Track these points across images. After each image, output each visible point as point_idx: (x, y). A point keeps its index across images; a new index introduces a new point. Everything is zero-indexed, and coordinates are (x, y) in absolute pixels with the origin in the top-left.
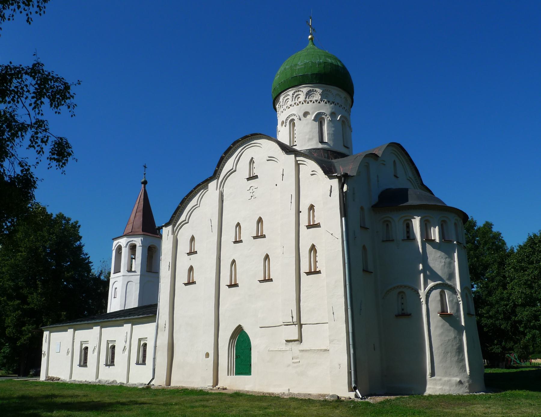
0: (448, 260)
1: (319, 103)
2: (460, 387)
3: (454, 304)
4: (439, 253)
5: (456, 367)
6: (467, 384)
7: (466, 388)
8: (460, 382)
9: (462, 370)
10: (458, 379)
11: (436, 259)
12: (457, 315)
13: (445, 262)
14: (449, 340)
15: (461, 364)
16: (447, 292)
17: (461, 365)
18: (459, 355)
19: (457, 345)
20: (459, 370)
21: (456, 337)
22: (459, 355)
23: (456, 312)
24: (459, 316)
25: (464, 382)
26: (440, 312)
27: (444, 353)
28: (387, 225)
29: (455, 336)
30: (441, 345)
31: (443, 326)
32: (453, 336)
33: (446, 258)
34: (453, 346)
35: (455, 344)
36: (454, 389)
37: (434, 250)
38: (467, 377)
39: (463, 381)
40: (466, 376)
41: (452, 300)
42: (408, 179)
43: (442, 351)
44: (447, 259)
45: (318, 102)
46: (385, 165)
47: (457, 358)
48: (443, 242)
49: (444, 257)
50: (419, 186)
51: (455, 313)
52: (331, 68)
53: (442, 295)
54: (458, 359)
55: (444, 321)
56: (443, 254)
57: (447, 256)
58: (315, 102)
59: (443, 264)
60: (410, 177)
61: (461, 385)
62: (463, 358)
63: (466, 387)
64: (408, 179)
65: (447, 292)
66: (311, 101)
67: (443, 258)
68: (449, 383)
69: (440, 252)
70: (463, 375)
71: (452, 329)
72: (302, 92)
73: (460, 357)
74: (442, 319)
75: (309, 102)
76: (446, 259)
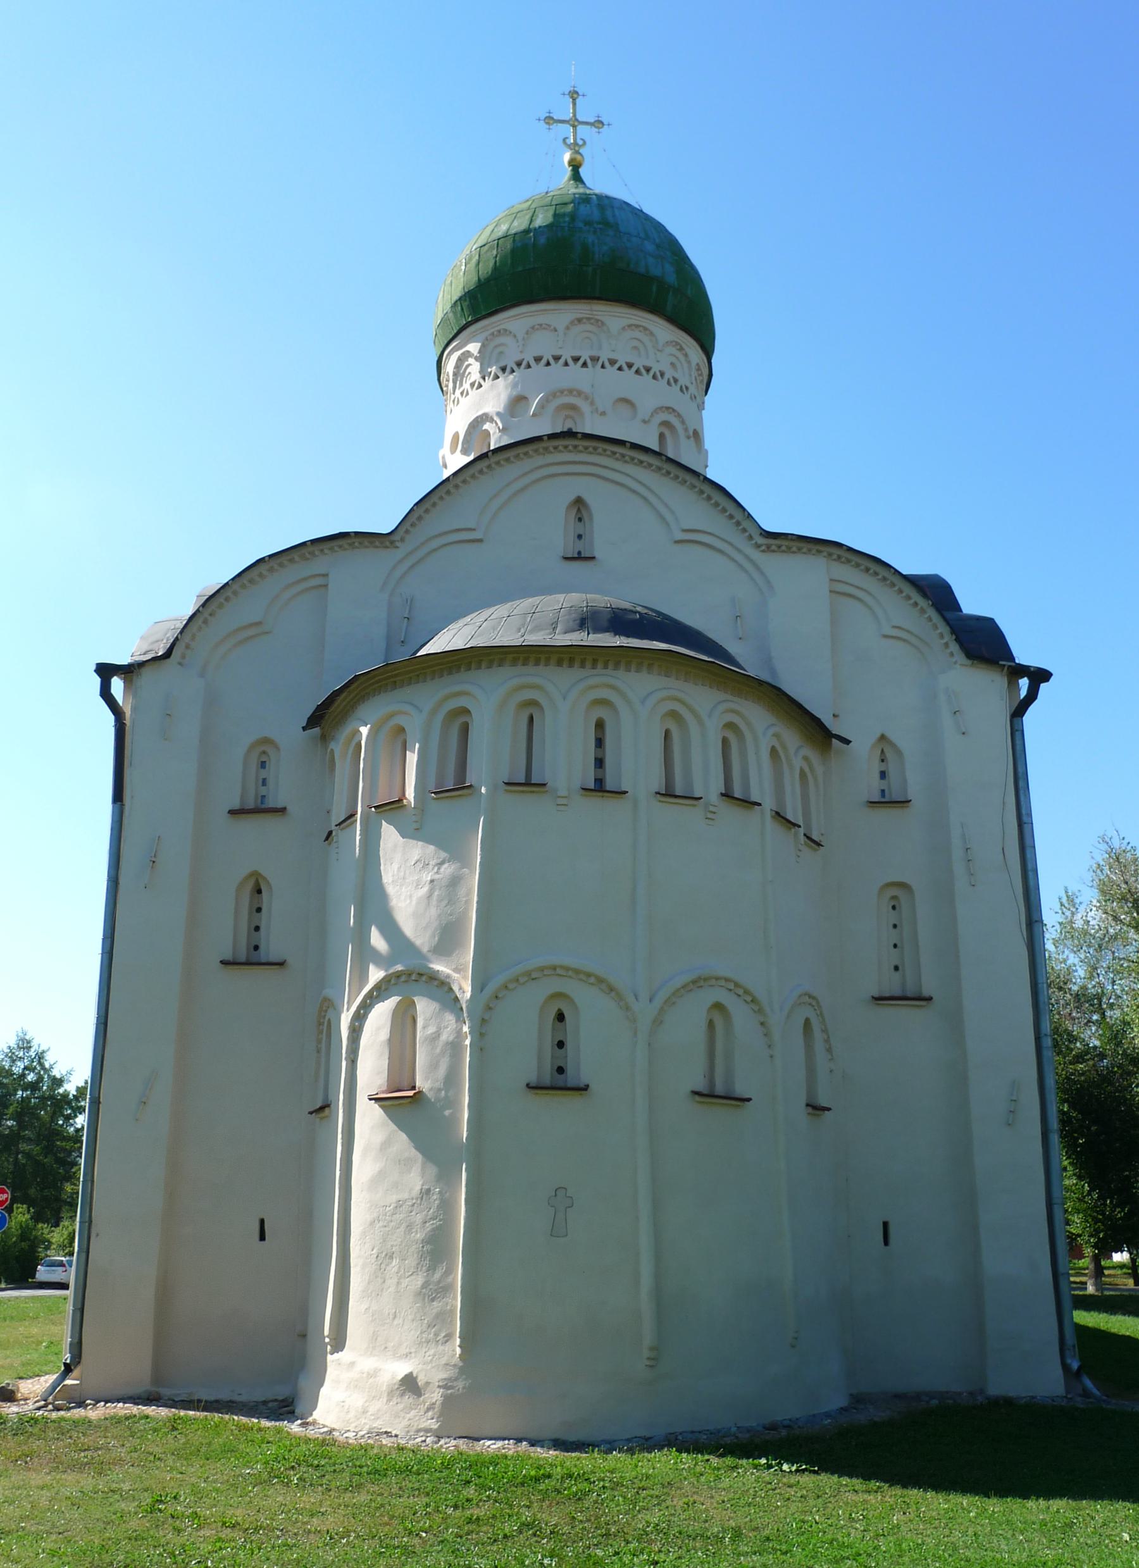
0: (448, 869)
2: (401, 1406)
3: (438, 1050)
4: (418, 850)
5: (410, 1317)
6: (435, 1396)
7: (430, 1414)
8: (410, 1385)
9: (436, 1335)
10: (401, 1369)
11: (404, 878)
12: (446, 1097)
13: (432, 881)
14: (399, 1204)
15: (437, 1305)
16: (424, 1007)
17: (435, 1311)
18: (432, 1269)
19: (428, 1224)
20: (421, 1333)
21: (428, 1191)
22: (432, 1269)
23: (444, 1084)
24: (453, 1103)
25: (428, 1383)
26: (385, 1088)
27: (377, 1257)
29: (426, 1187)
30: (372, 1223)
31: (385, 1145)
32: (418, 1188)
33: (442, 863)
34: (410, 1227)
35: (419, 1218)
36: (379, 1410)
37: (405, 840)
38: (447, 1364)
39: (421, 1381)
40: (444, 1361)
41: (437, 1036)
42: (677, 542)
43: (373, 1250)
44: (446, 865)
46: (480, 541)
47: (419, 1281)
48: (435, 799)
49: (432, 863)
50: (758, 546)
51: (439, 1090)
52: (496, 257)
53: (404, 1019)
54: (425, 1285)
55: (393, 1127)
56: (432, 848)
57: (443, 855)
59: (426, 889)
61: (408, 1399)
62: (450, 1279)
63: (428, 1410)
64: (677, 542)
65: (424, 1007)
68: (371, 1380)
69: (420, 843)
70: (431, 1352)
71: (420, 1156)
73: (437, 1276)
74: (387, 1118)
76: (439, 869)
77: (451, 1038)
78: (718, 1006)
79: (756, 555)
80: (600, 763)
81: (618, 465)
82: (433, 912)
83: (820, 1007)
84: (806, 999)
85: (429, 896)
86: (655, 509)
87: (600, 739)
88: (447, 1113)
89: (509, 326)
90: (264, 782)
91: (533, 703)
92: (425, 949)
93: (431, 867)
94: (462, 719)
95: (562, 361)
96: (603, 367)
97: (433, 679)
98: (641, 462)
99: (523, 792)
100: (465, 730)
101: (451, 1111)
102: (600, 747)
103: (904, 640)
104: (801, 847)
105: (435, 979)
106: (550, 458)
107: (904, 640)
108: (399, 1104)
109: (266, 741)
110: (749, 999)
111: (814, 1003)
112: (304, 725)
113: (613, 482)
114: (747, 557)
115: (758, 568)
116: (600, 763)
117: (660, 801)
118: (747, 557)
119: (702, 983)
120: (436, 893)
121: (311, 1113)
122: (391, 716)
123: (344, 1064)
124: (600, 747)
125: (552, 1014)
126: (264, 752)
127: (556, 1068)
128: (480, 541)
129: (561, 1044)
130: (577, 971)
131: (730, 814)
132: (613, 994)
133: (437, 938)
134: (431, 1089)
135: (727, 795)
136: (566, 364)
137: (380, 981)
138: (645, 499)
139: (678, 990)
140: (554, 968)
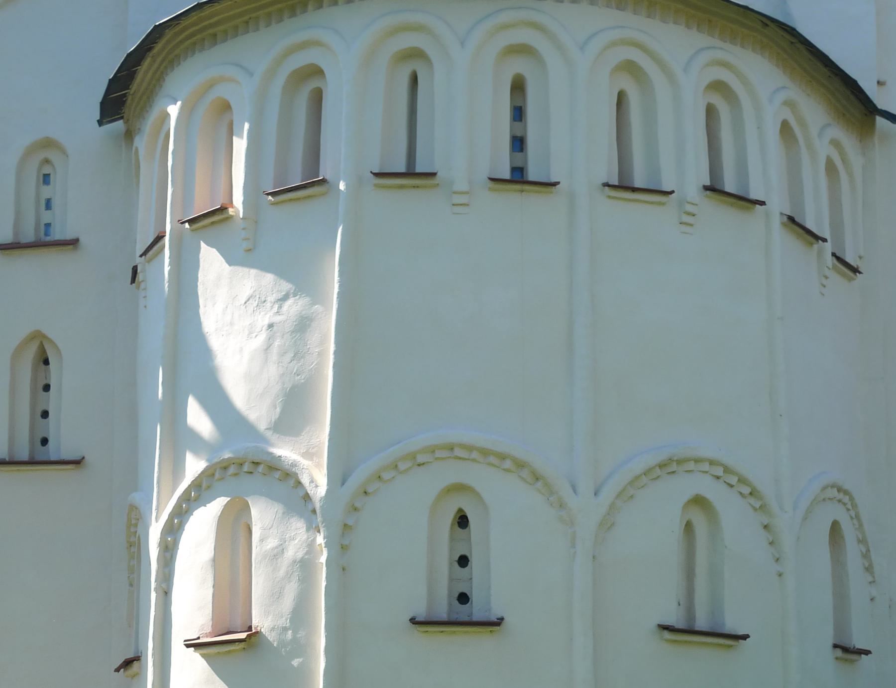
0: (293, 307)
3: (282, 573)
11: (231, 324)
12: (295, 640)
13: (271, 326)
23: (292, 620)
24: (301, 647)
26: (209, 629)
33: (285, 298)
37: (232, 268)
41: (280, 551)
44: (290, 301)
48: (273, 204)
49: (271, 298)
51: (285, 629)
56: (269, 277)
57: (286, 286)
59: (263, 337)
67: (268, 305)
69: (253, 272)
76: (280, 307)
77: (300, 555)
78: (699, 501)
80: (519, 143)
82: (273, 371)
83: (855, 506)
84: (834, 493)
85: (268, 348)
87: (521, 107)
88: (296, 662)
90: (48, 205)
91: (416, 54)
92: (262, 426)
93: (268, 305)
94: (313, 84)
97: (268, 25)
99: (402, 187)
100: (317, 98)
101: (301, 660)
102: (521, 120)
104: (828, 273)
105: (277, 469)
108: (229, 652)
109: (48, 144)
110: (746, 490)
111: (846, 499)
112: (98, 118)
116: (519, 143)
117: (609, 197)
119: (674, 467)
120: (277, 343)
121: (117, 670)
122: (211, 85)
123: (153, 595)
124: (521, 120)
125: (450, 516)
126: (47, 161)
127: (457, 595)
129: (463, 561)
130: (485, 452)
131: (712, 209)
132: (539, 484)
133: (278, 410)
134: (273, 629)
135: (713, 189)
137: (200, 475)
139: (637, 478)
140: (451, 448)
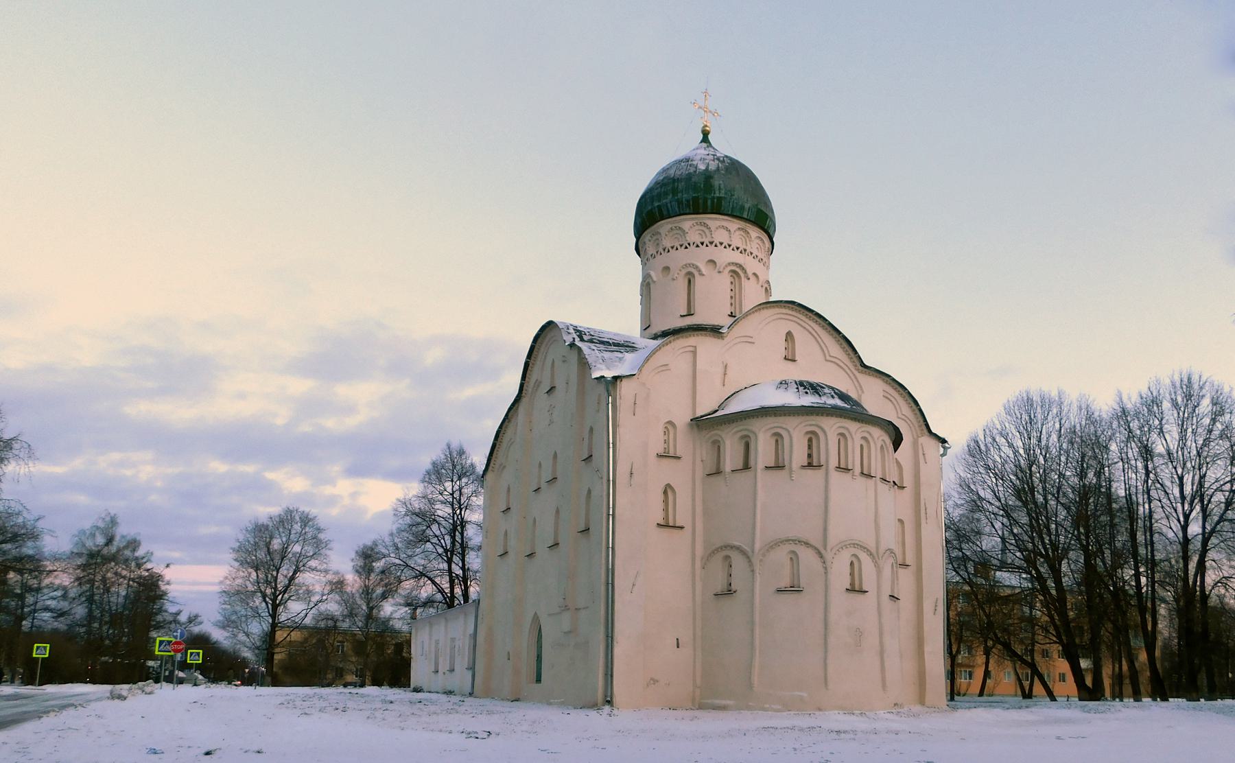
1: (686, 248)
28: (719, 447)
45: (684, 246)
46: (753, 343)
58: (679, 247)
60: (830, 356)
66: (672, 247)
72: (660, 234)
75: (670, 249)
79: (856, 373)
81: (807, 320)
86: (819, 344)
89: (710, 223)
95: (714, 244)
96: (733, 250)
98: (816, 321)
103: (905, 421)
106: (794, 313)
107: (905, 421)
113: (799, 324)
114: (853, 373)
115: (856, 378)
118: (853, 373)
128: (753, 343)
136: (725, 247)
138: (815, 338)
